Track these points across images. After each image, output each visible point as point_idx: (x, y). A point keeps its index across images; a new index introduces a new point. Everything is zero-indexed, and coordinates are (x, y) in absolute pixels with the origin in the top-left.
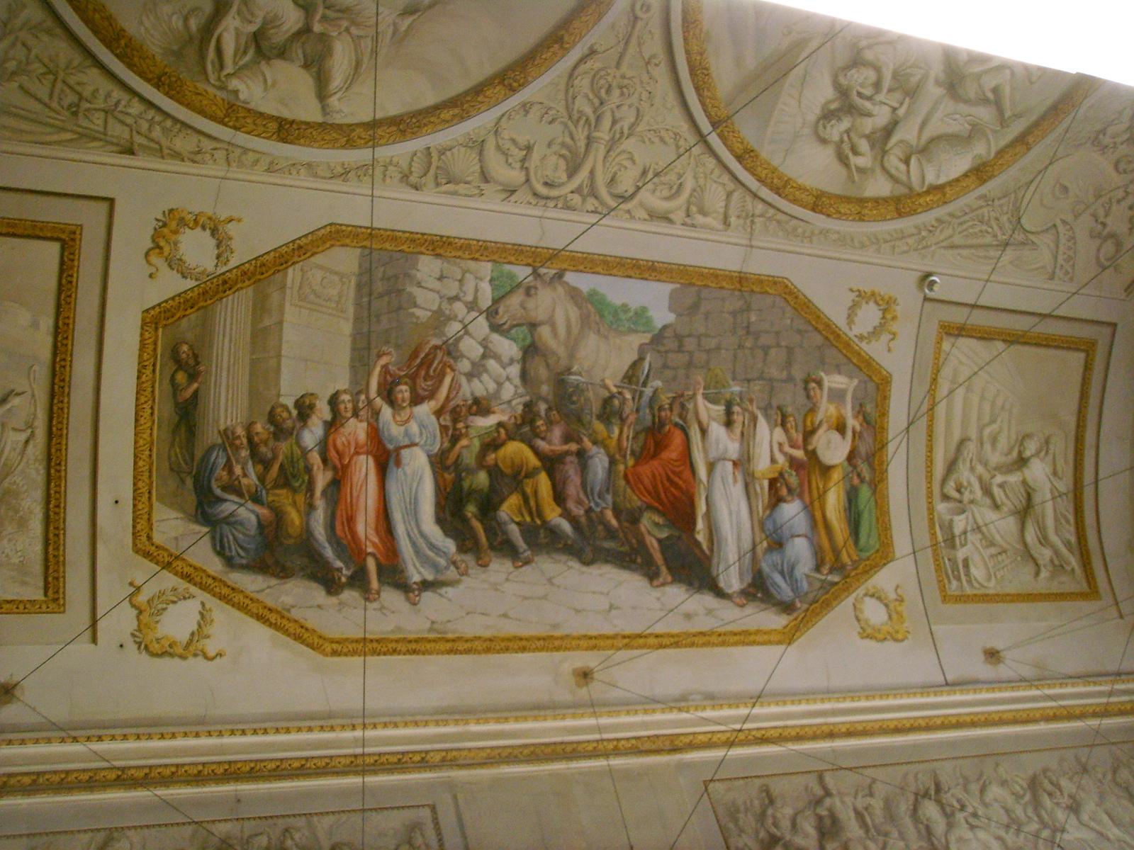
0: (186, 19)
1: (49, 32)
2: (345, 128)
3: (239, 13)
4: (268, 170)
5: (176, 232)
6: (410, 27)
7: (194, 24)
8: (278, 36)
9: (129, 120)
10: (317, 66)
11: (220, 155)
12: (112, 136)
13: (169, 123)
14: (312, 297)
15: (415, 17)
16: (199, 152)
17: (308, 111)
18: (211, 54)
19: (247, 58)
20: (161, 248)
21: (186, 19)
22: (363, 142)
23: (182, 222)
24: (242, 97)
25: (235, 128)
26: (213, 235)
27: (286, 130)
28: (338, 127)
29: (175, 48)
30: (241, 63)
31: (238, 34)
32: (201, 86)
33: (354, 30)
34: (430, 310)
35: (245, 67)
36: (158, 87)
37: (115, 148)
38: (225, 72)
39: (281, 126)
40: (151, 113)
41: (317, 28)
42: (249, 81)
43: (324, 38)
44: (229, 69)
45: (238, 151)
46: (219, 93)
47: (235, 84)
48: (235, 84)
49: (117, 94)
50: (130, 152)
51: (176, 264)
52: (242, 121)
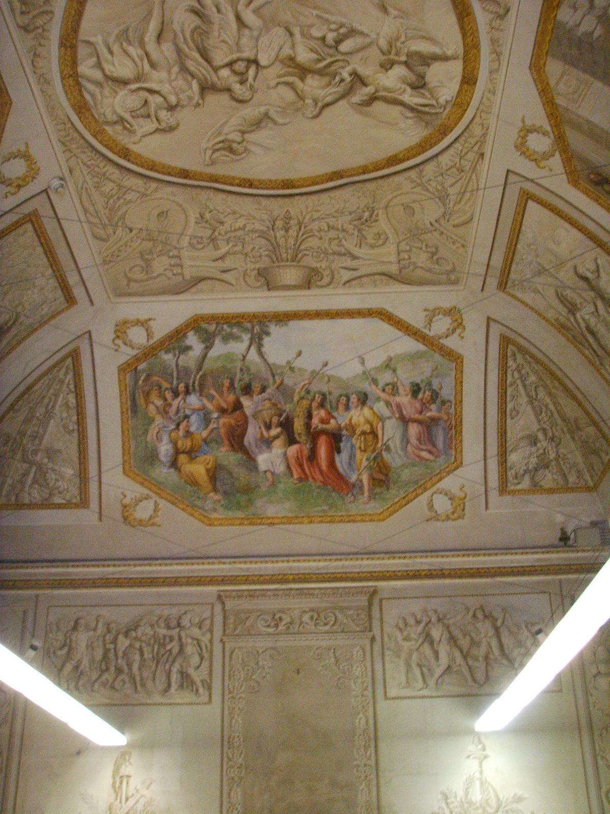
0: (407, 118)
1: (422, 171)
2: (467, 49)
3: (401, 94)
4: (494, 94)
5: (528, 149)
6: (396, 9)
7: (410, 115)
8: (411, 77)
9: (465, 151)
10: (428, 60)
11: (484, 115)
12: (474, 159)
13: (466, 134)
14: (576, 96)
15: (388, 7)
16: (483, 125)
17: (457, 68)
18: (426, 109)
19: (427, 94)
20: (536, 160)
21: (407, 118)
22: (475, 39)
23: (523, 144)
24: (450, 99)
25: (468, 105)
26: (532, 133)
27: (469, 80)
28: (466, 53)
29: (424, 124)
30: (429, 96)
31: (411, 96)
32: (444, 116)
33: (403, 39)
34: (597, 26)
35: (431, 94)
36: (446, 135)
37: (480, 161)
38: (436, 105)
39: (467, 83)
40: (461, 140)
41: (404, 58)
42: (440, 95)
43: (410, 55)
44: (434, 102)
45: (482, 107)
46: (448, 110)
47: (442, 101)
48: (442, 101)
49: (451, 151)
50: (482, 155)
51: (547, 156)
52: (465, 102)
